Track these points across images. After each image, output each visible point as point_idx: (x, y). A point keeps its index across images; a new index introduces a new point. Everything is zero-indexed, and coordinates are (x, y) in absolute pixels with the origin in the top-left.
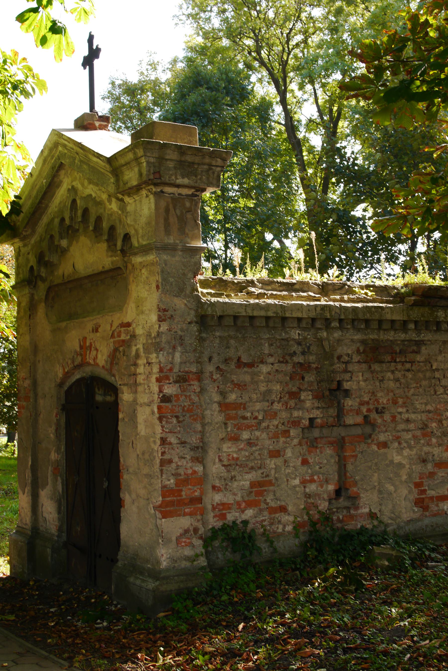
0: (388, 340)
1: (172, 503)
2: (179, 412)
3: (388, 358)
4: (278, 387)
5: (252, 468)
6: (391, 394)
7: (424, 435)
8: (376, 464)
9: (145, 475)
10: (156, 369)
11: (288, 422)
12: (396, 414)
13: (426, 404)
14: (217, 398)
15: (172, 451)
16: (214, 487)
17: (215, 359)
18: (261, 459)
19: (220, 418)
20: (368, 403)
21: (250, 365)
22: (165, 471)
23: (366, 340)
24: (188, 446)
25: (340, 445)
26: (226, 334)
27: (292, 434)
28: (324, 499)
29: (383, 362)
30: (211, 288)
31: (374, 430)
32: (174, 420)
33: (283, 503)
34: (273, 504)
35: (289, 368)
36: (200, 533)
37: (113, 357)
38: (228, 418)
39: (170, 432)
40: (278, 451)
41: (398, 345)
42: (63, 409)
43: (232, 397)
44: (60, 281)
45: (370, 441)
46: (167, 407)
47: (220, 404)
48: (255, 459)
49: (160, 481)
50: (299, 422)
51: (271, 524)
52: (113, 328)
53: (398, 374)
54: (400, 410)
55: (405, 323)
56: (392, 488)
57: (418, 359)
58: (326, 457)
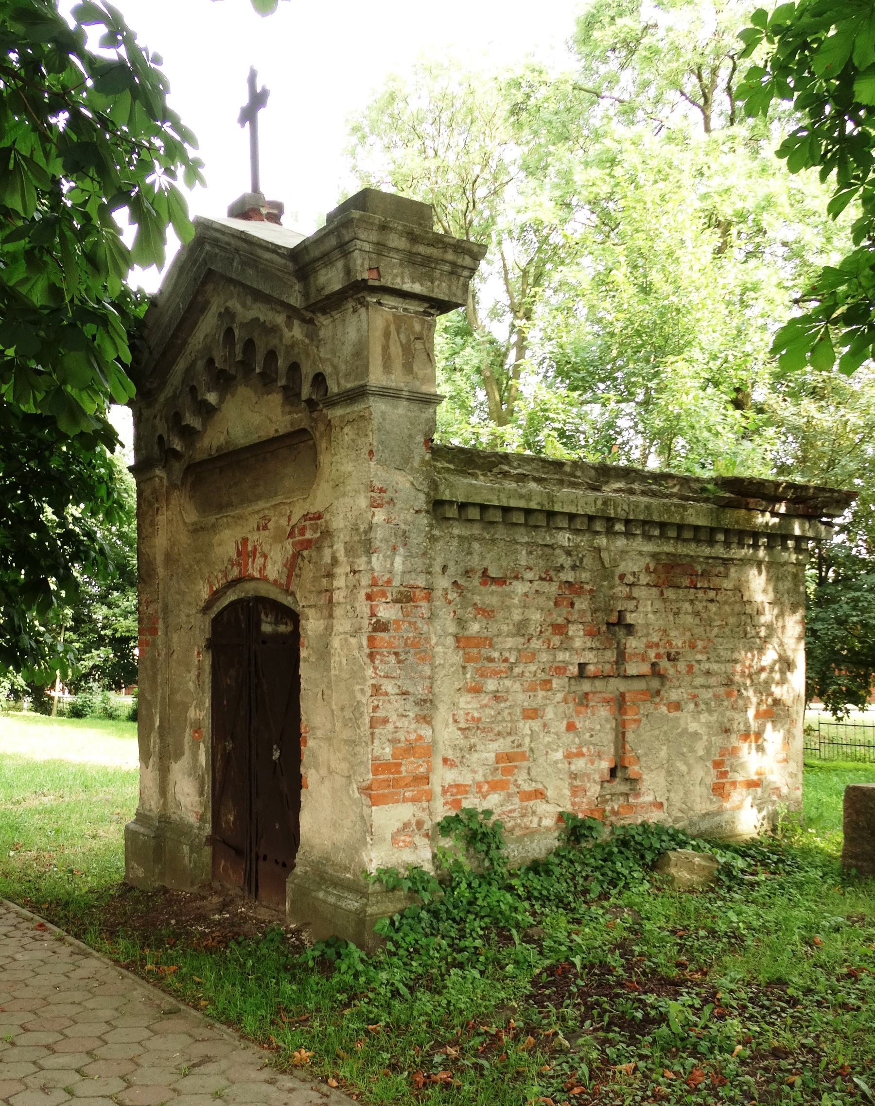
0: (687, 556)
1: (387, 783)
2: (398, 647)
3: (686, 582)
4: (538, 616)
5: (499, 734)
6: (688, 634)
8: (665, 732)
9: (345, 741)
10: (365, 581)
11: (551, 667)
12: (694, 663)
14: (452, 628)
15: (388, 706)
16: (445, 761)
17: (452, 569)
18: (512, 721)
19: (456, 658)
20: (657, 645)
21: (500, 581)
22: (377, 735)
23: (659, 553)
24: (412, 699)
25: (620, 703)
26: (469, 533)
27: (554, 686)
28: (595, 781)
29: (679, 587)
30: (449, 462)
31: (663, 684)
32: (392, 659)
33: (540, 786)
34: (526, 787)
35: (552, 589)
36: (425, 827)
37: (292, 566)
38: (468, 659)
39: (387, 677)
41: (700, 563)
43: (475, 628)
45: (657, 700)
46: (382, 639)
47: (457, 638)
48: (504, 720)
49: (370, 750)
50: (565, 669)
51: (523, 816)
52: (292, 523)
53: (699, 606)
54: (699, 657)
56: (684, 768)
57: (725, 586)
58: (599, 721)
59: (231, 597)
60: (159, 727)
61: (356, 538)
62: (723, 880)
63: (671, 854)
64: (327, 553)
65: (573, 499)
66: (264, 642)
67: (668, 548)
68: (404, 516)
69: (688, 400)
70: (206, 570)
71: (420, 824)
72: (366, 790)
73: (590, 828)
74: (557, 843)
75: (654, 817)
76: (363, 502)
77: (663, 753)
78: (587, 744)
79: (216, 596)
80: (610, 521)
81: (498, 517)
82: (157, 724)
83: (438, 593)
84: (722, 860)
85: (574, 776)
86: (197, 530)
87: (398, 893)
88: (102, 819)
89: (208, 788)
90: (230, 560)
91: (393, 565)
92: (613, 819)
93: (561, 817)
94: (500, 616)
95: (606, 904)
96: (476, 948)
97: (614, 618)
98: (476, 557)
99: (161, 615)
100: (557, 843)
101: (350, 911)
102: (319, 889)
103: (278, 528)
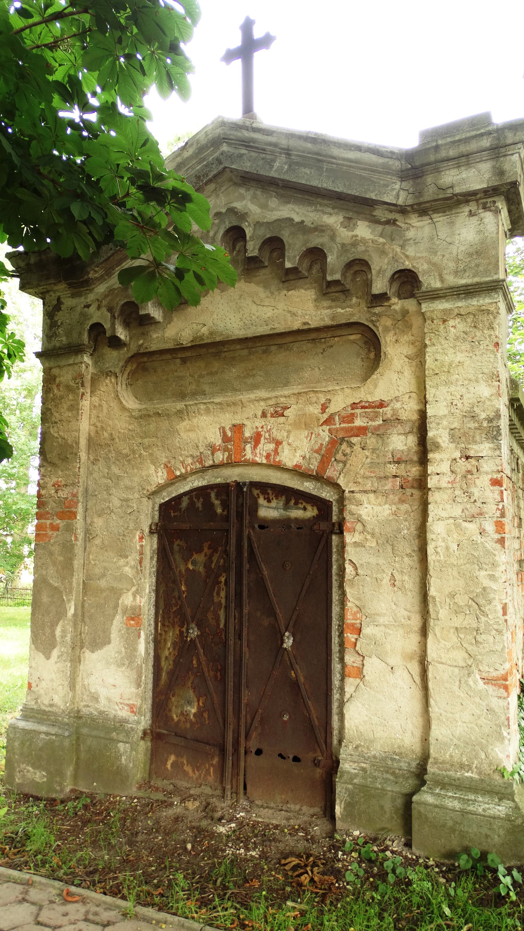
60: (75, 615)
66: (261, 527)
82: (71, 611)
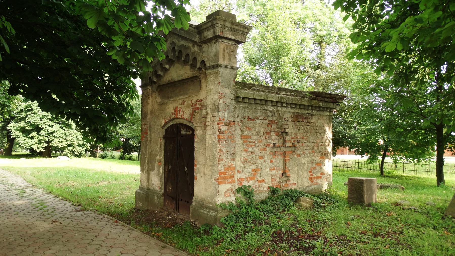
3: (301, 120)
5: (252, 163)
7: (313, 152)
10: (217, 119)
13: (314, 140)
14: (240, 133)
15: (223, 155)
16: (238, 171)
17: (240, 116)
19: (241, 142)
20: (294, 138)
21: (253, 120)
25: (284, 155)
32: (224, 141)
34: (260, 179)
35: (266, 122)
37: (192, 115)
38: (244, 142)
39: (223, 147)
40: (262, 157)
42: (163, 138)
43: (246, 133)
44: (164, 83)
48: (254, 159)
51: (259, 187)
52: (193, 102)
53: (305, 127)
54: (305, 141)
55: (308, 106)
56: (301, 173)
58: (279, 159)
59: (171, 123)
61: (214, 107)
62: (315, 205)
63: (301, 198)
64: (204, 112)
65: (272, 97)
67: (297, 111)
68: (228, 101)
69: (288, 69)
70: (164, 116)
71: (232, 190)
72: (217, 180)
73: (277, 191)
74: (268, 195)
75: (294, 187)
76: (216, 97)
77: (296, 169)
78: (276, 166)
79: (166, 123)
80: (282, 103)
81: (252, 101)
83: (236, 123)
84: (315, 200)
85: (272, 176)
86: (161, 104)
87: (226, 210)
88: (124, 189)
89: (163, 179)
90: (172, 113)
91: (225, 115)
92: (283, 188)
93: (269, 187)
94: (253, 129)
95: (285, 213)
96: (251, 226)
97: (283, 131)
98: (247, 113)
99: (149, 128)
100: (268, 195)
101: (212, 216)
102: (201, 209)
103: (188, 104)
